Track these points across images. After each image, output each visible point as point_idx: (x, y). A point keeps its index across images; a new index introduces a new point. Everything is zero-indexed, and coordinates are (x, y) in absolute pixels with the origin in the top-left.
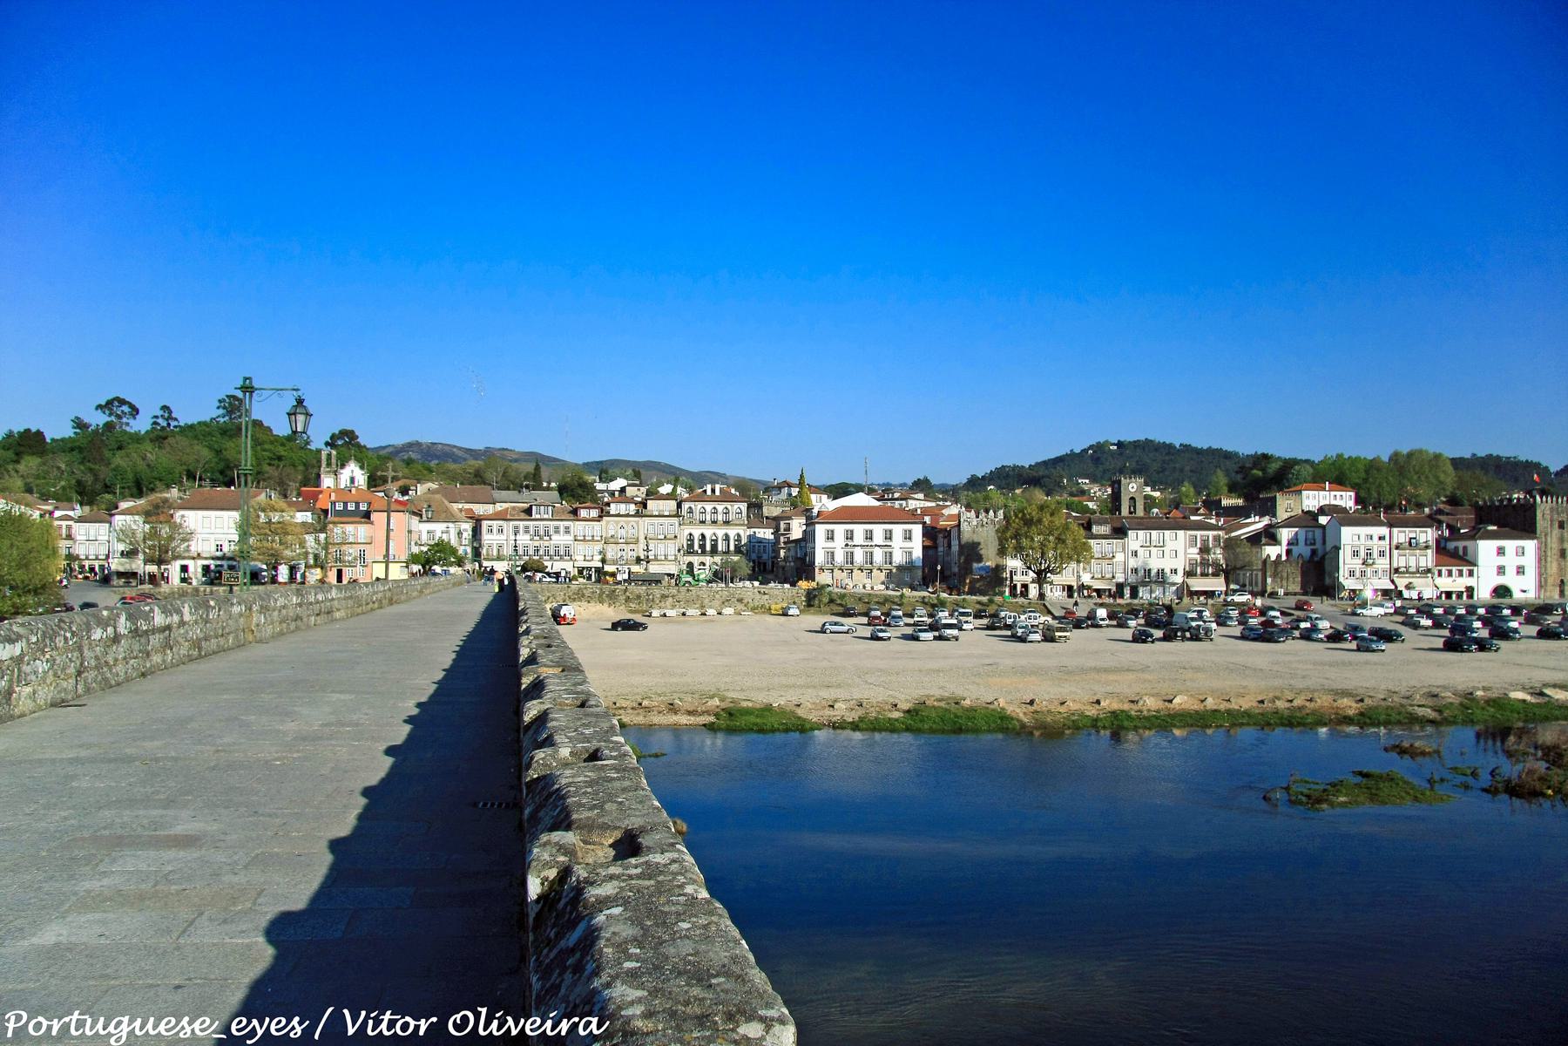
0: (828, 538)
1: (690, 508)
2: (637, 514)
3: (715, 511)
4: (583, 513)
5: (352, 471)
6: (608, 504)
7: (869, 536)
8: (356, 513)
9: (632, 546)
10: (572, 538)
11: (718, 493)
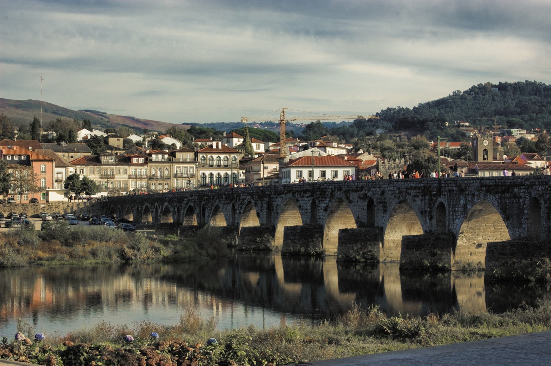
1: (203, 157)
2: (170, 161)
3: (227, 159)
4: (135, 161)
6: (150, 155)
8: (21, 162)
9: (166, 182)
10: (126, 176)
11: (220, 147)
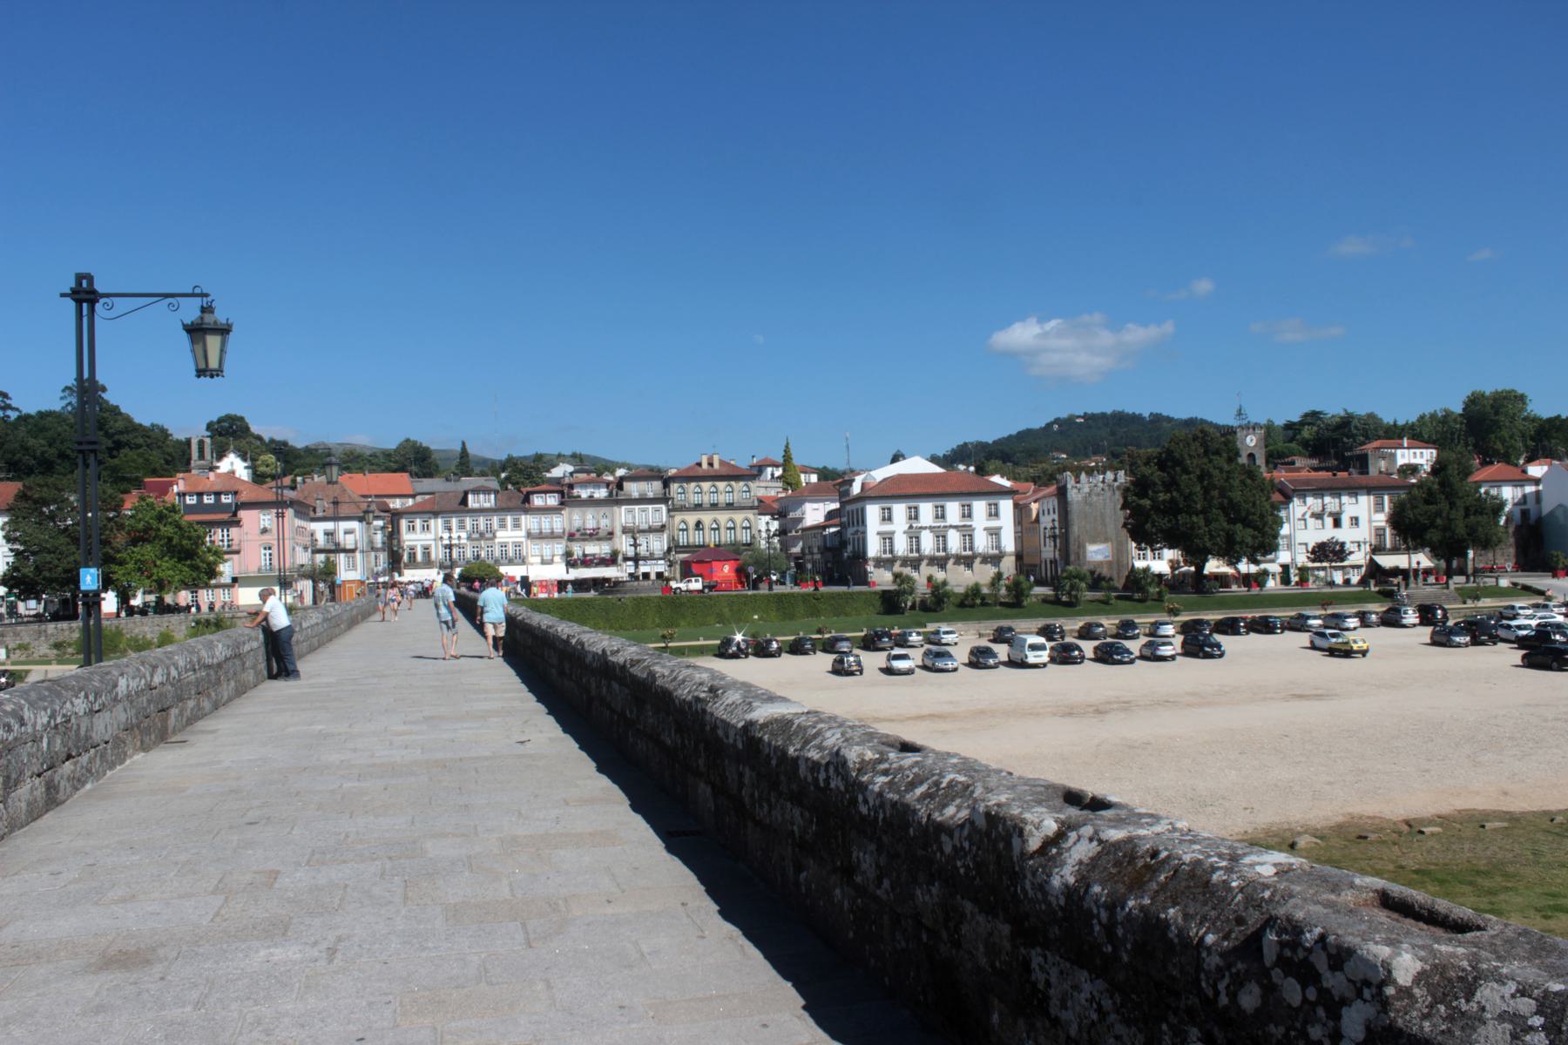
0: (884, 519)
4: (537, 501)
5: (232, 464)
7: (941, 515)
10: (523, 533)
